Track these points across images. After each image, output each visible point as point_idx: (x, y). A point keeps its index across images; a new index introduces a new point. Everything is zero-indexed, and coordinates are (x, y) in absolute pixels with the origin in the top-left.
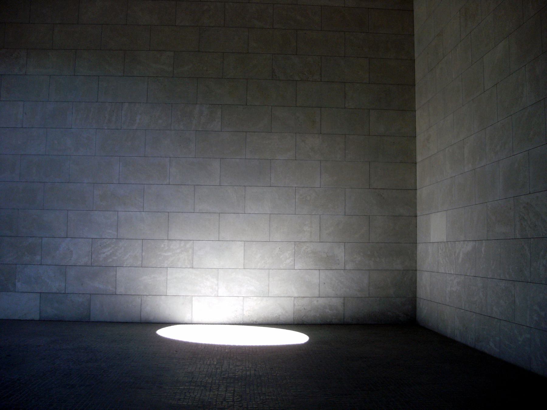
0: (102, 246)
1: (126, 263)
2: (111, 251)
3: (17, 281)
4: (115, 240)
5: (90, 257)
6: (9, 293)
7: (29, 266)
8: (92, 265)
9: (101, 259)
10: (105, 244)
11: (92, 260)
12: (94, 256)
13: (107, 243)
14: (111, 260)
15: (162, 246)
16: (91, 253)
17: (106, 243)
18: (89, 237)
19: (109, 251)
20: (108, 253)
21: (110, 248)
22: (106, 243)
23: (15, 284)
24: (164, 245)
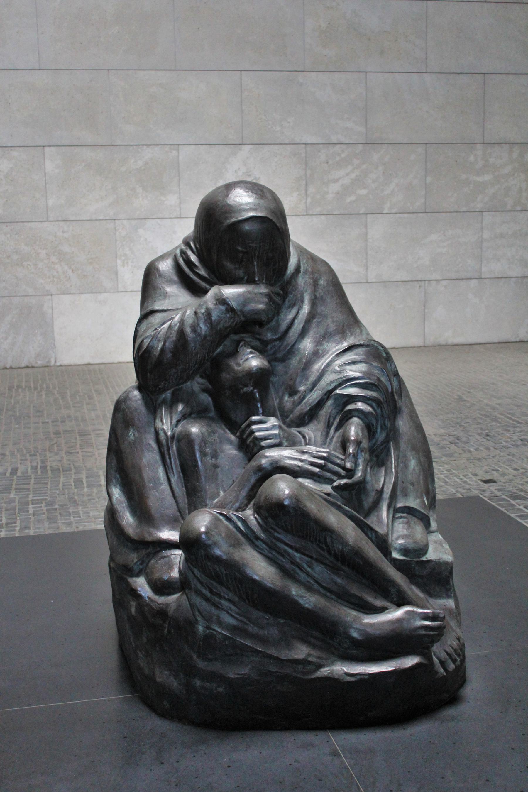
0: (331, 162)
1: (388, 205)
2: (353, 176)
3: (119, 262)
4: (360, 147)
5: (304, 192)
6: (102, 297)
7: (149, 223)
8: (310, 213)
9: (330, 197)
10: (338, 158)
11: (309, 200)
12: (311, 190)
13: (343, 156)
14: (353, 198)
15: (472, 158)
16: (304, 182)
17: (339, 154)
18: (298, 140)
19: (347, 175)
20: (347, 181)
21: (350, 168)
22: (339, 154)
23: (116, 273)
24: (475, 155)
